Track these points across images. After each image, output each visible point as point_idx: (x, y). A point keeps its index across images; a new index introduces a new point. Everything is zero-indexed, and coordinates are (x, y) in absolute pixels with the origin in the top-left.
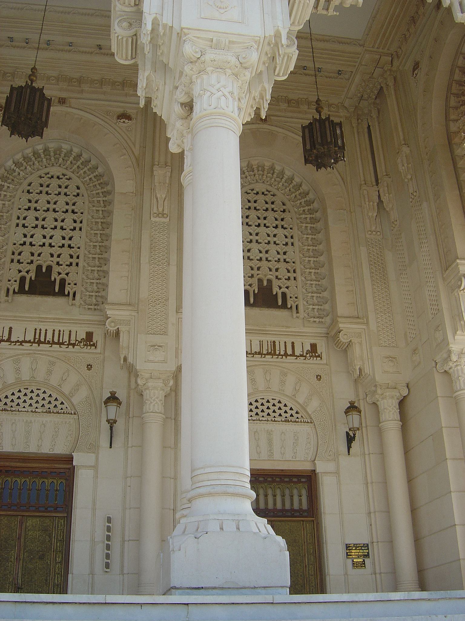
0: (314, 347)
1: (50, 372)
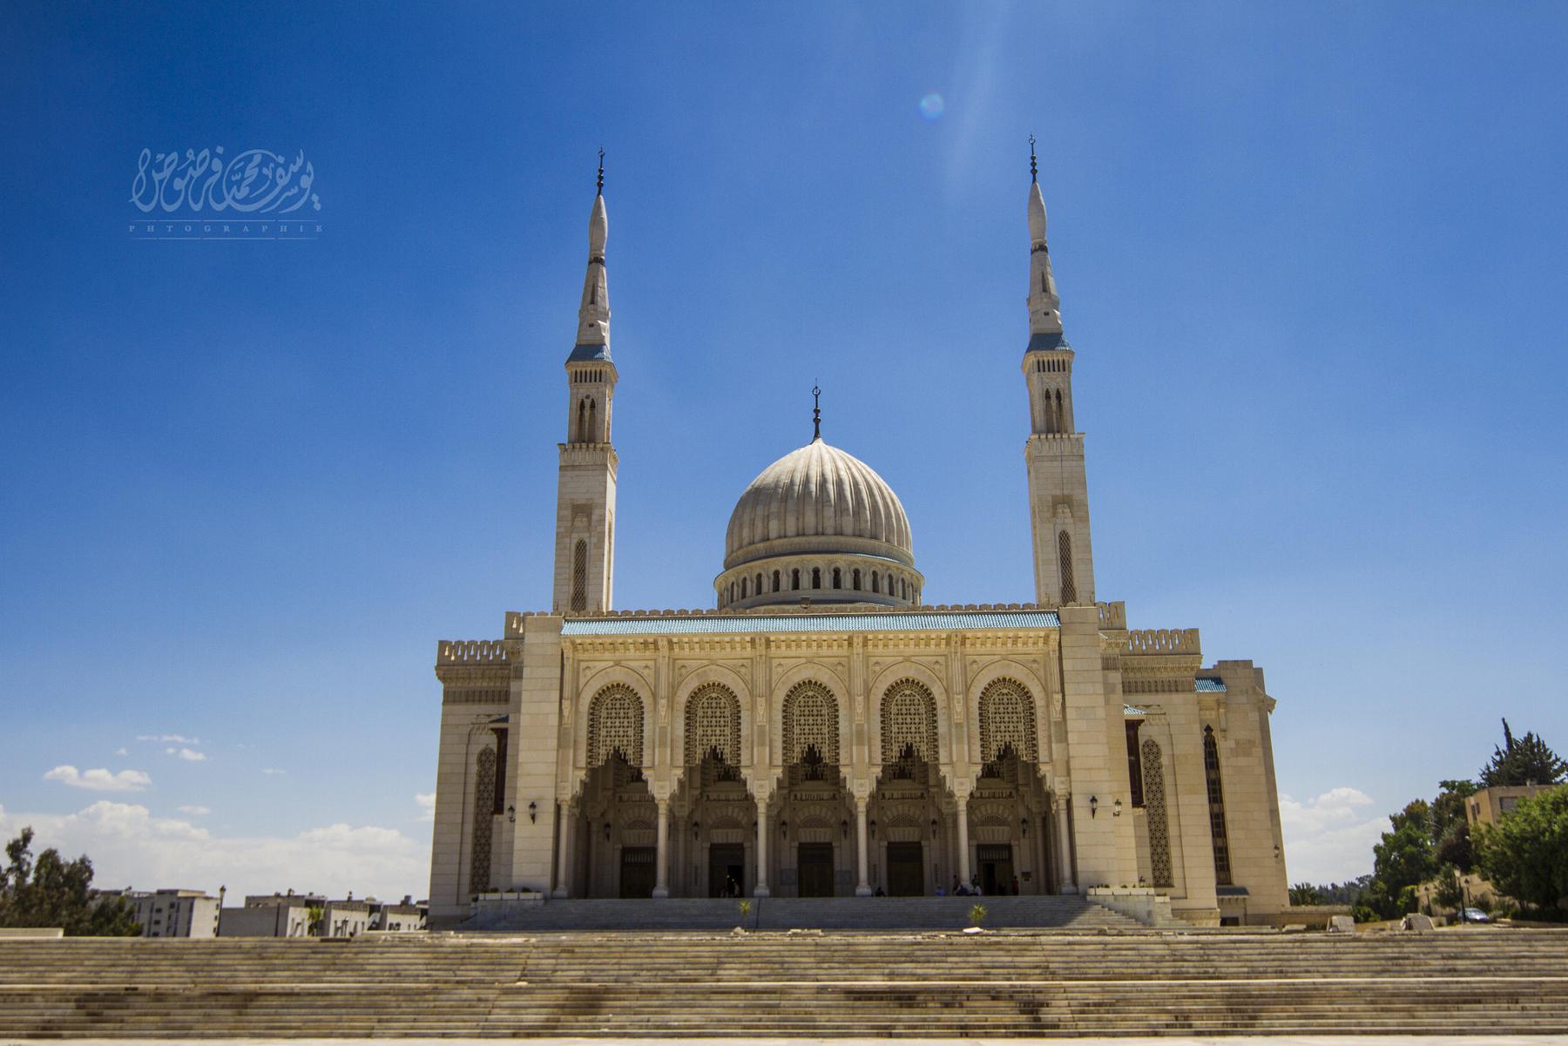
0: (1011, 793)
1: (909, 811)
